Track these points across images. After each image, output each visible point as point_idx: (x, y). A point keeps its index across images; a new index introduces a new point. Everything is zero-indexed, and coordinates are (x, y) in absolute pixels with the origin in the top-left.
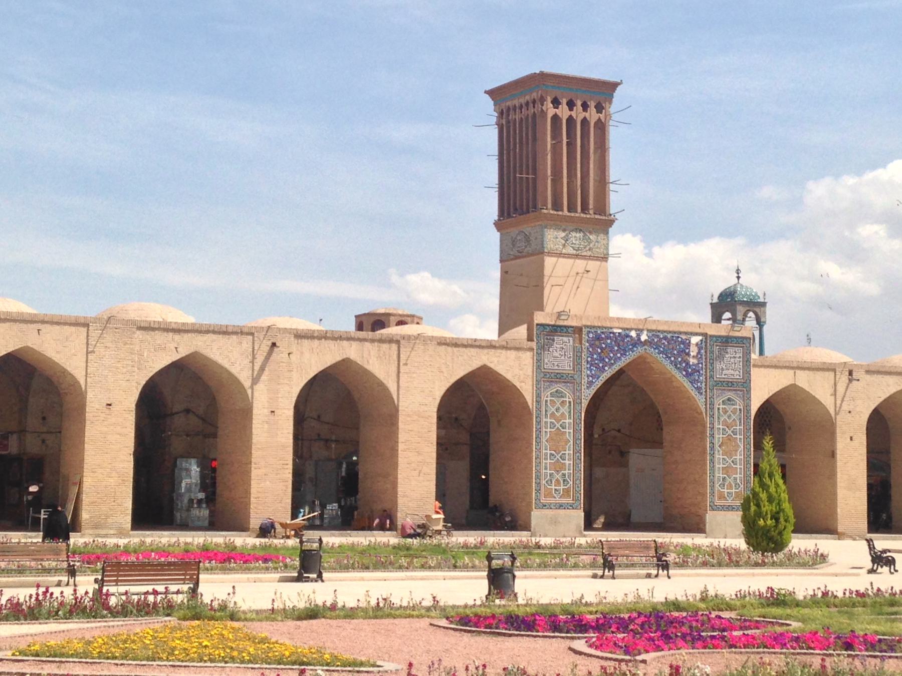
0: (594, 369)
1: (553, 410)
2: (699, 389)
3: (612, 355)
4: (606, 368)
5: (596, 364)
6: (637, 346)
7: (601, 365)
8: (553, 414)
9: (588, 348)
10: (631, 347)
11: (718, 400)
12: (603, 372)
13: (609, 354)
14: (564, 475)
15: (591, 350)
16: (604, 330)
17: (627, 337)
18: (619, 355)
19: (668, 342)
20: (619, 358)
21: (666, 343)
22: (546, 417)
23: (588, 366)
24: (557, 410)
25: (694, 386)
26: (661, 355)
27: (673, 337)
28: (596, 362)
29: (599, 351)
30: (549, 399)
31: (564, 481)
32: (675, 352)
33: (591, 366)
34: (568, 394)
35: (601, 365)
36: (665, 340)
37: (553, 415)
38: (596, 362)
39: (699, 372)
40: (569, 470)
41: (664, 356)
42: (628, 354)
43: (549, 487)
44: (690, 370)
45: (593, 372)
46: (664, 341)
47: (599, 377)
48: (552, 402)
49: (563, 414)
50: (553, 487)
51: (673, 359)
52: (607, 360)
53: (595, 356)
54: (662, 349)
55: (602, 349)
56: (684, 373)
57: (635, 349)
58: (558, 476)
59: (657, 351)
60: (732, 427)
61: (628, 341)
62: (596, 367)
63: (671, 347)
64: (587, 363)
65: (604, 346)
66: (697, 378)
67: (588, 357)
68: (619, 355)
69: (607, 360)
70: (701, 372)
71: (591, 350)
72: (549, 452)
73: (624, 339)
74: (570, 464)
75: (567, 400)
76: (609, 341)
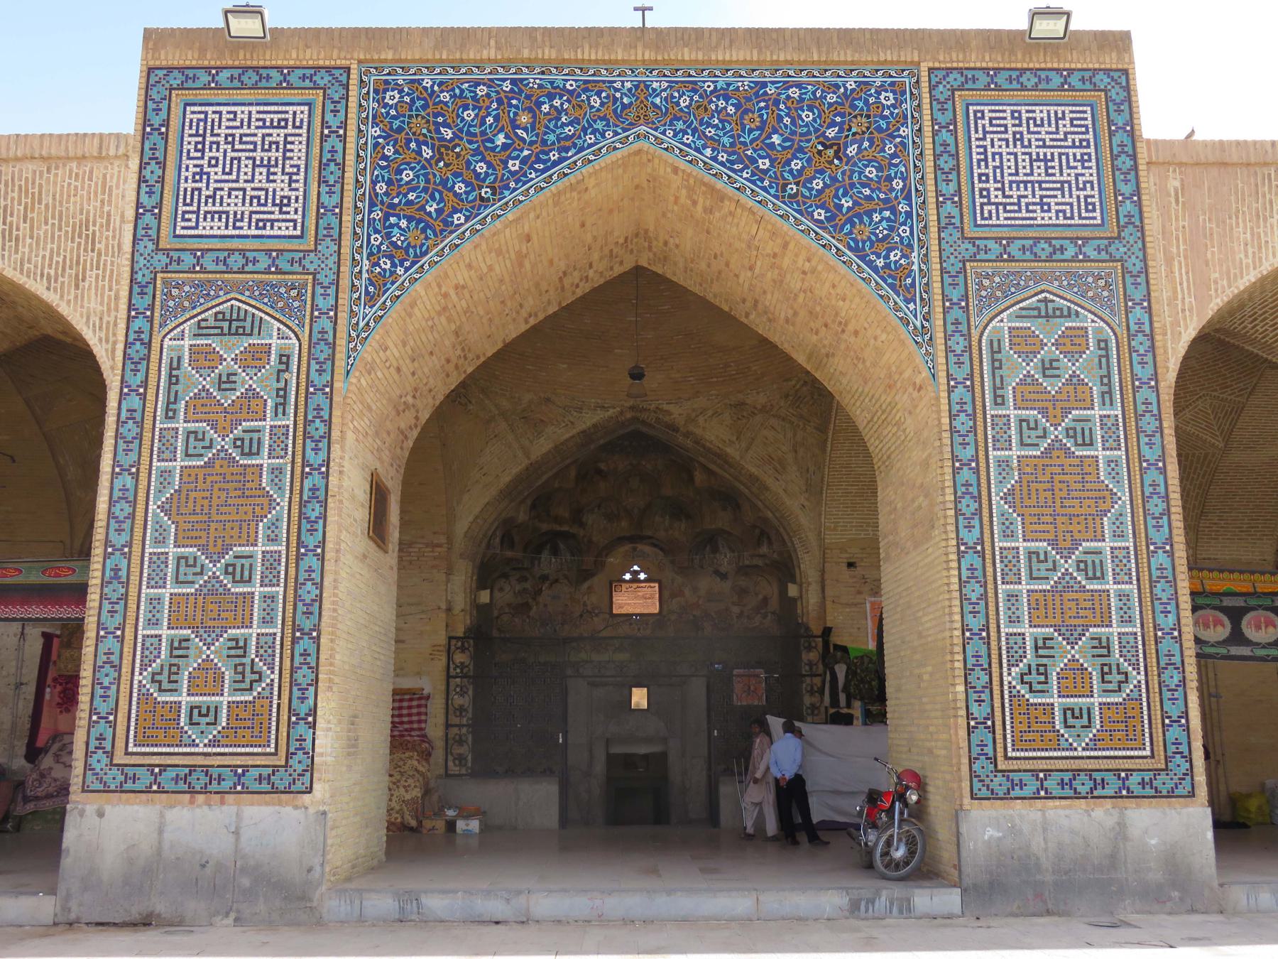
0: (404, 223)
1: (208, 382)
2: (897, 279)
3: (481, 168)
4: (458, 218)
5: (410, 203)
6: (599, 125)
7: (432, 208)
8: (202, 404)
9: (376, 145)
10: (569, 130)
11: (988, 313)
12: (440, 234)
13: (468, 163)
14: (239, 647)
15: (389, 151)
16: (451, 75)
17: (551, 97)
18: (514, 165)
19: (736, 106)
20: (520, 177)
21: (731, 110)
22: (170, 414)
23: (377, 215)
24: (225, 383)
25: (870, 264)
26: (708, 152)
27: (764, 85)
28: (411, 196)
29: (427, 152)
30: (187, 343)
31: (239, 670)
32: (776, 139)
33: (387, 216)
34: (277, 324)
35: (432, 208)
36: (727, 98)
37: (202, 404)
38: (411, 196)
39: (894, 210)
40: (264, 622)
41: (723, 157)
42: (554, 156)
43: (162, 698)
44: (847, 203)
45: (396, 236)
46: (722, 103)
47: (424, 254)
48: (204, 358)
49: (251, 394)
50: (185, 699)
51: (764, 164)
52: (460, 188)
53: (407, 176)
54: (710, 132)
55: (442, 148)
56: (820, 214)
57: (590, 139)
58: (216, 653)
59: (688, 139)
60: (1066, 412)
61: (559, 111)
62: (410, 219)
63: (753, 120)
64: (372, 205)
65: (448, 134)
66: (882, 230)
67: (374, 183)
68: (514, 165)
69: (460, 188)
70: (902, 207)
71: (389, 151)
72: (172, 551)
73: (541, 104)
74: (265, 597)
75: (274, 342)
76: (469, 115)
